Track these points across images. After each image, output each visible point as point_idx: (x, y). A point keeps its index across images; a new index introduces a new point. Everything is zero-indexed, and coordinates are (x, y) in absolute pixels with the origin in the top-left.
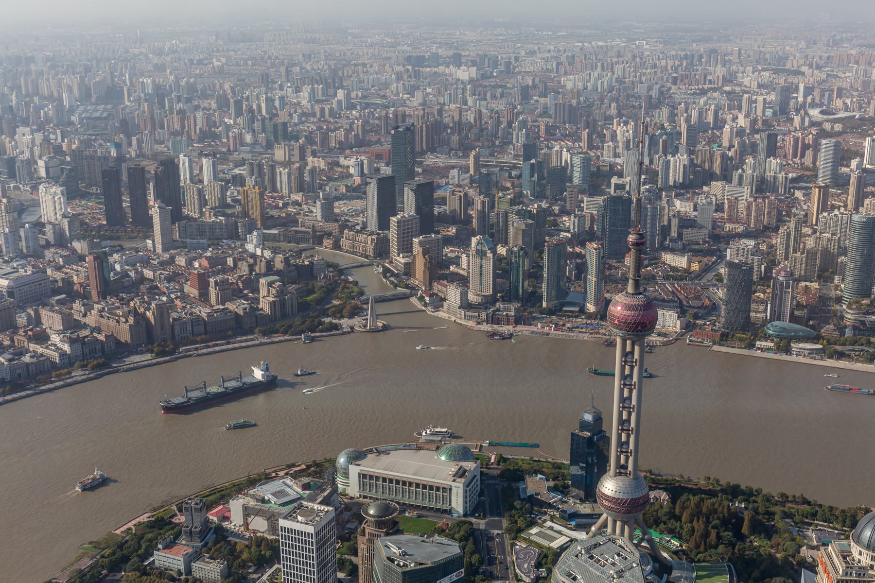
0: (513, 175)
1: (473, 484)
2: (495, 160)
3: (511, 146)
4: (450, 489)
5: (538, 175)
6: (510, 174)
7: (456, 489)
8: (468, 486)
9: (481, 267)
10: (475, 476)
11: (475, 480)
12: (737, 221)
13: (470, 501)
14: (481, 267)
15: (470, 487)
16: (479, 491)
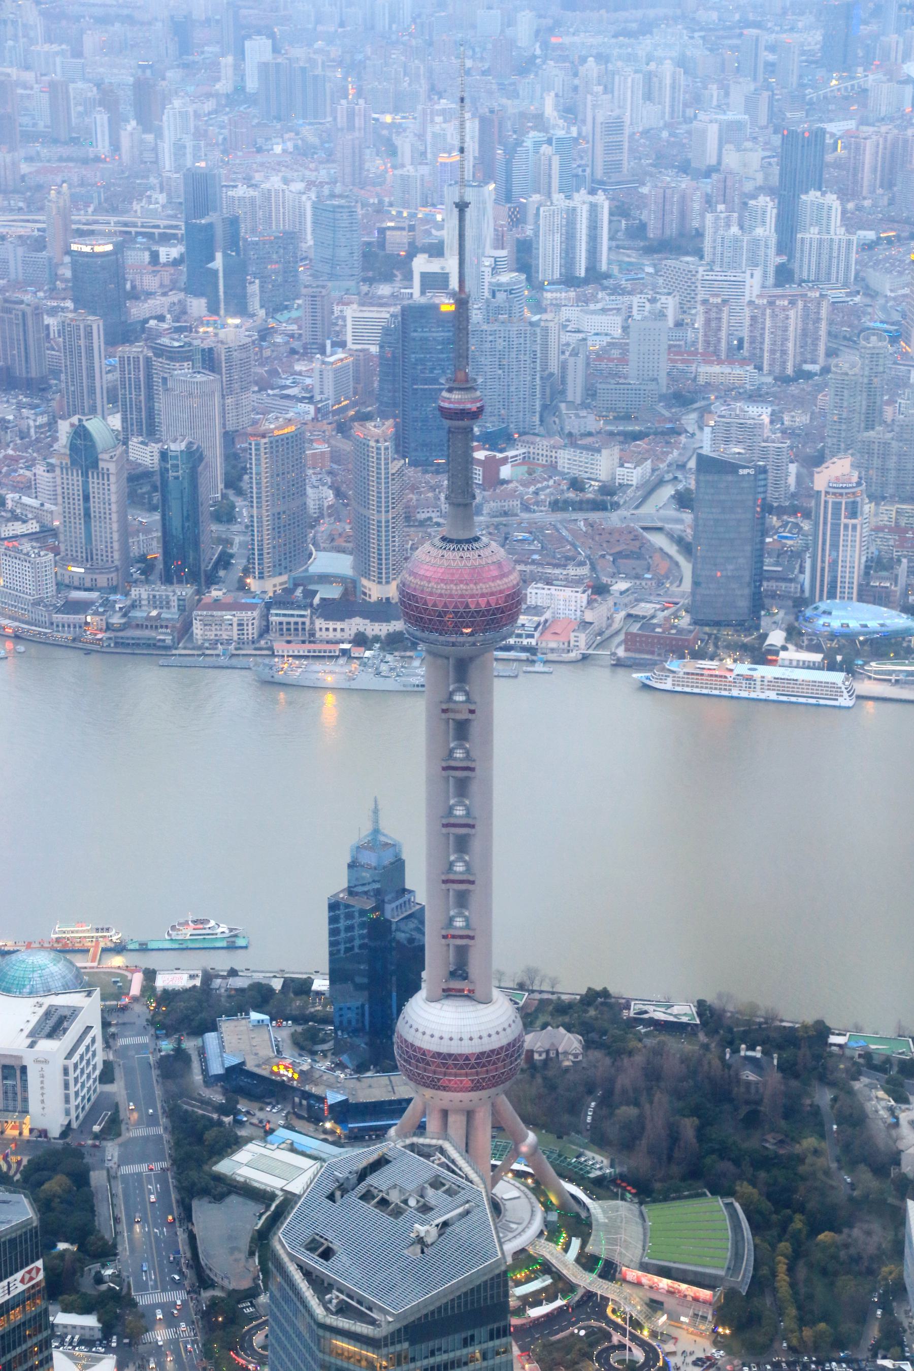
0: (163, 259)
1: (82, 1049)
2: (113, 219)
3: (153, 180)
4: (24, 1069)
5: (225, 255)
6: (155, 256)
7: (40, 1066)
8: (69, 1056)
9: (86, 498)
10: (89, 1028)
11: (88, 1040)
12: (735, 354)
13: (77, 1094)
14: (86, 498)
15: (76, 1058)
16: (100, 1067)
